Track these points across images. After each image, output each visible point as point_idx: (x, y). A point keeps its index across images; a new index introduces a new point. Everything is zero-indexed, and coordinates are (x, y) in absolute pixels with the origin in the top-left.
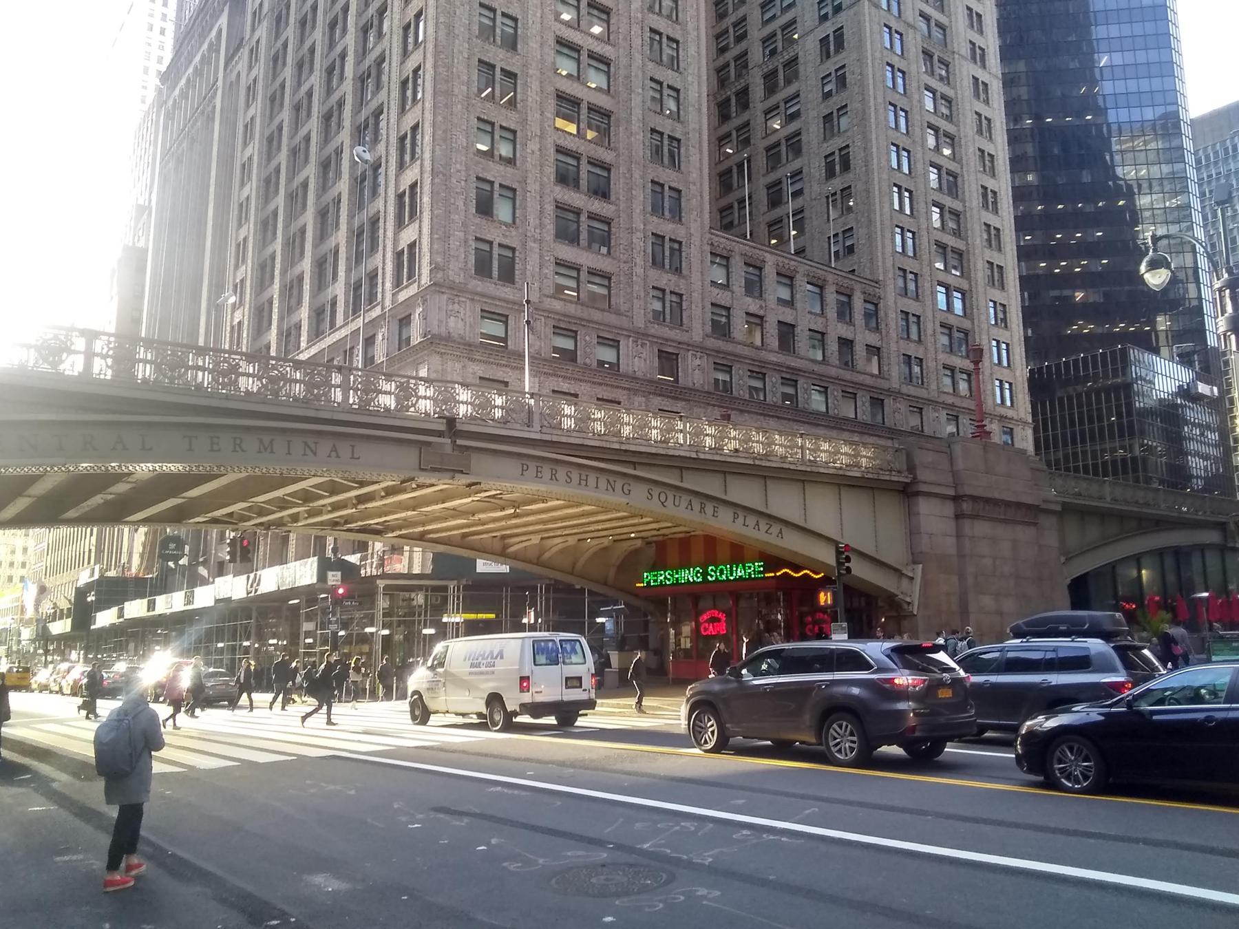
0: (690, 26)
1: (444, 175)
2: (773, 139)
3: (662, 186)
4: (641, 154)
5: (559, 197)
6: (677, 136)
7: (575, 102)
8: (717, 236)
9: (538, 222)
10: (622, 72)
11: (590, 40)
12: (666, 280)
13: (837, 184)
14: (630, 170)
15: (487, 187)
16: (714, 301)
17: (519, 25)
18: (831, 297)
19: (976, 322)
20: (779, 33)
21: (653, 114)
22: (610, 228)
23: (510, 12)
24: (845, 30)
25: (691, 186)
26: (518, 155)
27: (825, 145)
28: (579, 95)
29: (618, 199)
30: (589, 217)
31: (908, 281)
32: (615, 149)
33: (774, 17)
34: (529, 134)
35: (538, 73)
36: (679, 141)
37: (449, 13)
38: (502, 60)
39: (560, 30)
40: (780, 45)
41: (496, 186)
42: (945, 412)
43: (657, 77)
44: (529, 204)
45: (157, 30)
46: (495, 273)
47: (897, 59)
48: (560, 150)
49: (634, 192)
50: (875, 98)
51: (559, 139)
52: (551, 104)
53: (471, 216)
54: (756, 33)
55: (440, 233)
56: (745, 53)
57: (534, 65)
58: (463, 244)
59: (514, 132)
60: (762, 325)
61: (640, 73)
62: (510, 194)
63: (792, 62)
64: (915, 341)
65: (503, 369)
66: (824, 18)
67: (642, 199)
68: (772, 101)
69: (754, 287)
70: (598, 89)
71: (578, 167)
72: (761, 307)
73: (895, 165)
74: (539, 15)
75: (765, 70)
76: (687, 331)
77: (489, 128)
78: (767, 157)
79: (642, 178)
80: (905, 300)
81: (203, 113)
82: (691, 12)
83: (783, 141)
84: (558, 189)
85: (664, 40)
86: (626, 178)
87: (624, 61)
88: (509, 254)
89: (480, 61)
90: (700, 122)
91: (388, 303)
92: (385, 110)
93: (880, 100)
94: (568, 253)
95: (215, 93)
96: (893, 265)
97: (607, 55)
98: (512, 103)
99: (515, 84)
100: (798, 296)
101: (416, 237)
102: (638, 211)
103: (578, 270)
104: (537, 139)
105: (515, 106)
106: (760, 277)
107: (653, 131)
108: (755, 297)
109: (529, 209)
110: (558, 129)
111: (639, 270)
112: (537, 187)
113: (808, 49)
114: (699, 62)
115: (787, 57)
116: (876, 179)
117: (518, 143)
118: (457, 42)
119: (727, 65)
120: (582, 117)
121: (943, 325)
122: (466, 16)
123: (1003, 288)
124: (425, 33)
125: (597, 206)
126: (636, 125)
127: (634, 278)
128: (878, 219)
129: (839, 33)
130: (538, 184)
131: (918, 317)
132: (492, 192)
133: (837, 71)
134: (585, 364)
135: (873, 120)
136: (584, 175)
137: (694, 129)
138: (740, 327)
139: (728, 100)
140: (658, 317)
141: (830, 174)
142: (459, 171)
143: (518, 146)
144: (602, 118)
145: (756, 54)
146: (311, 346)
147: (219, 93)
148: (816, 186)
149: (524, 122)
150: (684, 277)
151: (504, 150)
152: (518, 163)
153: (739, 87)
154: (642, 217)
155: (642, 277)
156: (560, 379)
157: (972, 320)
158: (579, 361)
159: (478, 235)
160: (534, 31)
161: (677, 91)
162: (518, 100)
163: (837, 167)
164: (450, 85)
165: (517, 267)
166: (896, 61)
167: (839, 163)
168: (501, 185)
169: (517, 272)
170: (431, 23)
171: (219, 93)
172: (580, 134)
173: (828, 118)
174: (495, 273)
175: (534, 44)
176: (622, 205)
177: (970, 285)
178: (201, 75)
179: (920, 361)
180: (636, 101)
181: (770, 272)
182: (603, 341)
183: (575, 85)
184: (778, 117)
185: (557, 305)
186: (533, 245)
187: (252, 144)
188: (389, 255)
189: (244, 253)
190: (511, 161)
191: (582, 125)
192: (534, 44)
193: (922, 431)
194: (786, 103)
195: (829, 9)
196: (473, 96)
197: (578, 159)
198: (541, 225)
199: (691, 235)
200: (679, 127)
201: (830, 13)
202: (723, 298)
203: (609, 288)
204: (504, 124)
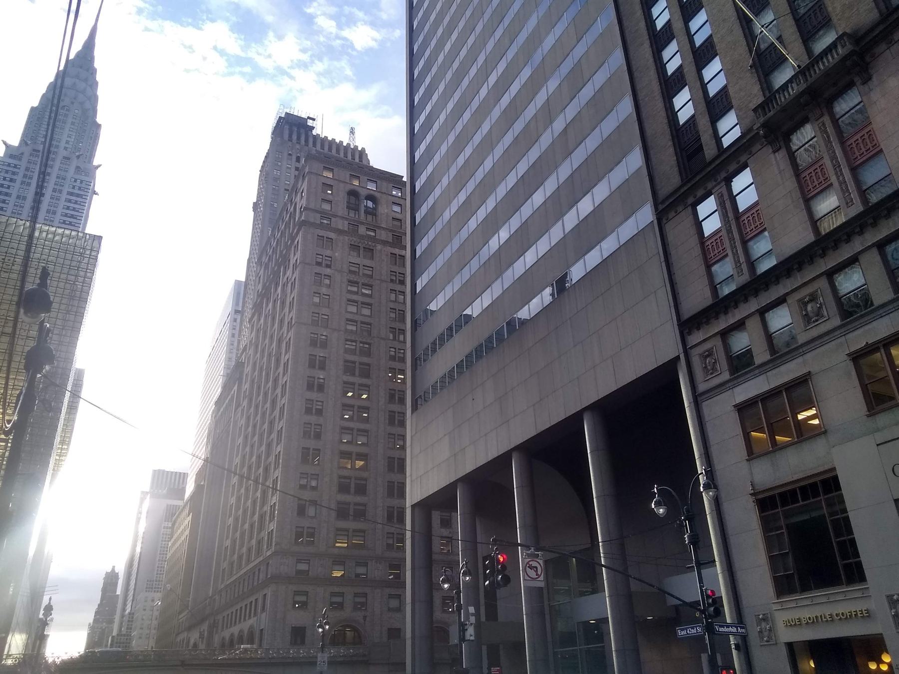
17: (323, 427)
26: (319, 485)
70: (363, 444)
72: (450, 532)
94: (342, 524)
95: (231, 422)
103: (348, 531)
107: (389, 458)
117: (319, 480)
127: (377, 530)
136: (353, 486)
151: (314, 483)
172: (353, 467)
182: (358, 564)
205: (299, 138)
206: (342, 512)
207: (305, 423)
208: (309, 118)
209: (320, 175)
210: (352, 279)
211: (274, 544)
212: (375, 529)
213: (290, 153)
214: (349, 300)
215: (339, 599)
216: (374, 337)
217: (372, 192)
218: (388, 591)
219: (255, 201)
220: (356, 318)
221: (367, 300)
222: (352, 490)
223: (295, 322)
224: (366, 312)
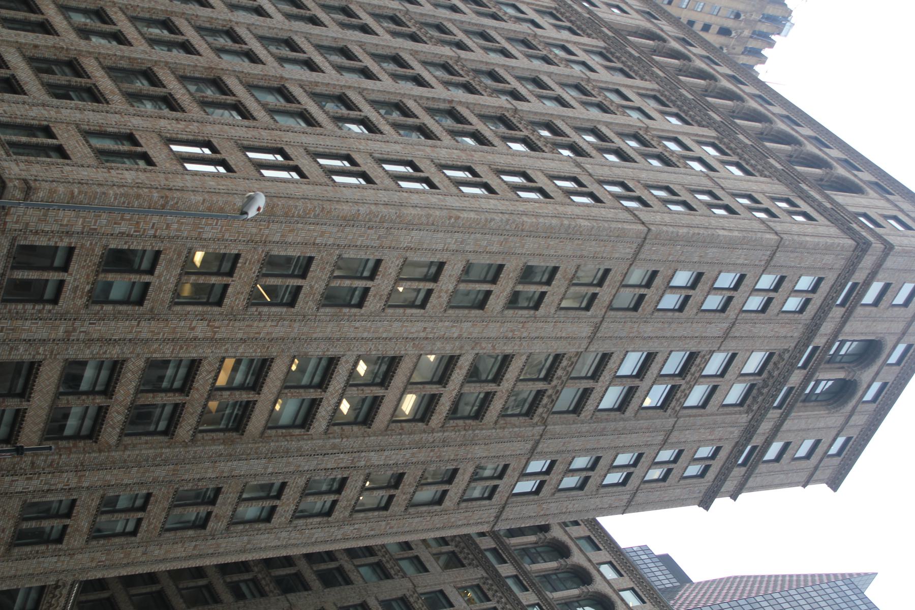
0: (348, 530)
1: (163, 206)
4: (186, 477)
5: (130, 365)
6: (211, 524)
7: (256, 386)
8: (70, 593)
9: (95, 336)
10: (294, 445)
11: (333, 401)
14: (166, 462)
15: (145, 265)
17: (354, 310)
21: (239, 488)
23: (370, 298)
25: (141, 550)
28: (265, 389)
29: (126, 448)
30: (100, 408)
32: (193, 440)
34: (216, 324)
35: (292, 335)
37: (370, 221)
38: (312, 287)
39: (347, 362)
41: (146, 278)
43: (287, 490)
44: (120, 324)
46: (20, 275)
48: (194, 365)
49: (135, 470)
51: (210, 364)
52: (256, 352)
53: (104, 242)
55: (82, 197)
57: (305, 329)
58: (65, 229)
61: (292, 468)
67: (126, 481)
74: (365, 335)
79: (155, 481)
82: (365, 529)
84: (141, 363)
85: (333, 497)
86: (154, 459)
87: (307, 445)
88: (49, 293)
89: (310, 259)
90: (227, 553)
92: (246, 122)
97: (316, 424)
99: (281, 304)
102: (108, 477)
104: (209, 334)
107: (218, 491)
109: (113, 323)
110: (222, 361)
111: (20, 484)
112: (145, 335)
114: (305, 545)
117: (205, 308)
118: (335, 230)
120: (237, 393)
122: (368, 243)
124: (345, 185)
125: (116, 417)
126: (225, 467)
130: (149, 335)
136: (160, 399)
137: (218, 546)
149: (233, 317)
150: (8, 550)
153: (263, 582)
154: (99, 483)
155: (12, 489)
159: (77, 251)
160: (346, 329)
161: (268, 519)
162: (261, 309)
164: (282, 219)
165: (29, 306)
168: (147, 285)
169: (20, 306)
170: (357, 194)
172: (215, 390)
174: (20, 275)
175: (330, 329)
176: (116, 455)
180: (257, 466)
183: (278, 384)
186: (62, 329)
191: (226, 394)
192: (330, 329)
196: (267, 249)
198: (90, 342)
199: (71, 555)
200: (222, 525)
204: (230, 290)
213: (742, 17)
216: (545, 423)
217: (860, 393)
222: (148, 399)
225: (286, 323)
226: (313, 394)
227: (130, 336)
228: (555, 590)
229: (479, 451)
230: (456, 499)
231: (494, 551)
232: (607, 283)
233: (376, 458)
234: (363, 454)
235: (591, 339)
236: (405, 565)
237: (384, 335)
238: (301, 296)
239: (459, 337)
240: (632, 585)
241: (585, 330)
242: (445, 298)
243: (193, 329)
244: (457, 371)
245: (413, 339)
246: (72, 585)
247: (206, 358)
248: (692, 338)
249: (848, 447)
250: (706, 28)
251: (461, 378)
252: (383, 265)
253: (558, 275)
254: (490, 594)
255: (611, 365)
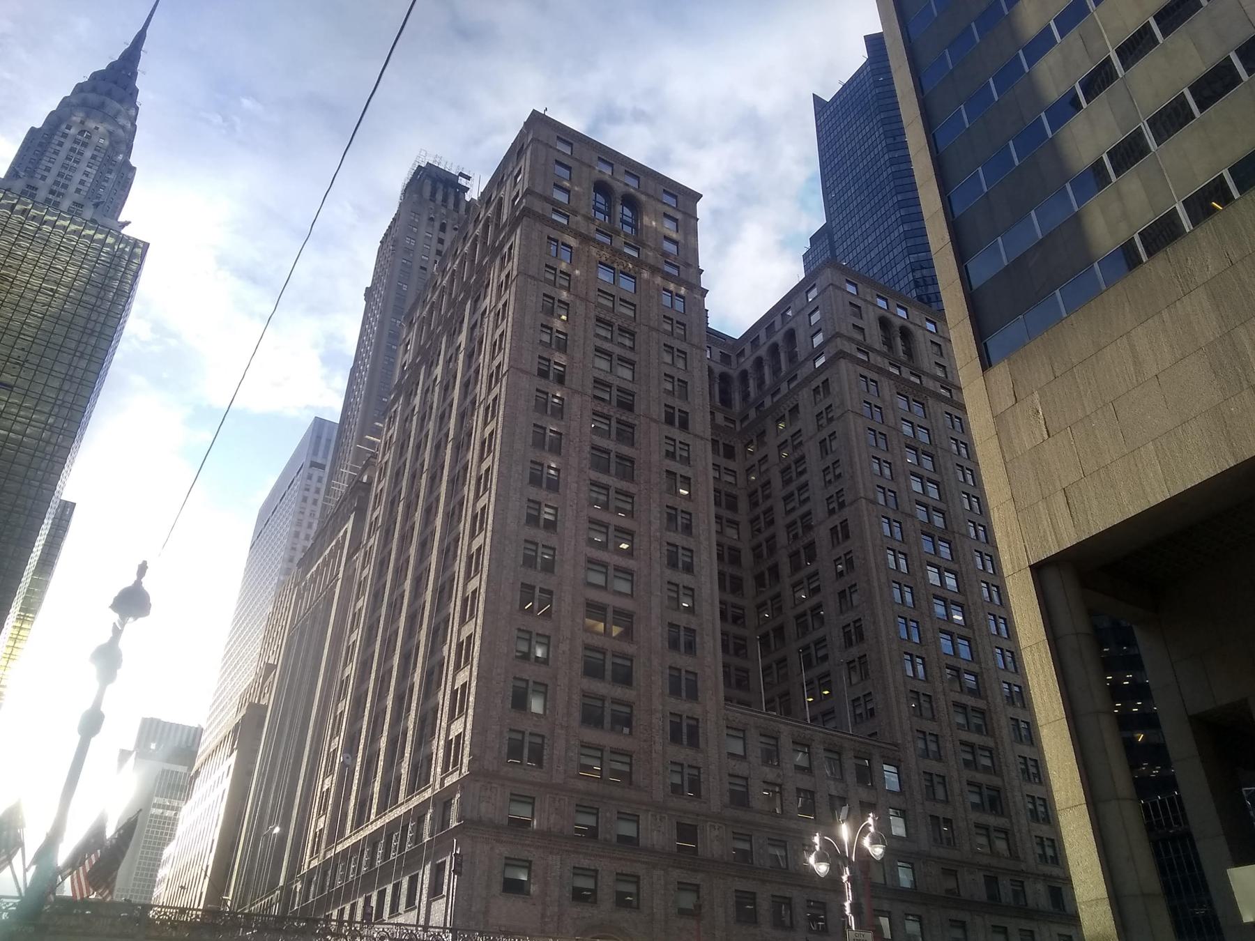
2: (800, 610)
3: (679, 670)
6: (693, 627)
12: (683, 754)
13: (855, 652)
16: (731, 772)
18: (849, 763)
19: (1006, 778)
20: (799, 521)
22: (632, 711)
24: (848, 522)
26: (551, 656)
27: (842, 617)
31: (928, 743)
33: (793, 509)
36: (694, 631)
40: (800, 531)
41: (531, 683)
42: (981, 874)
45: (310, 501)
47: (897, 543)
49: (653, 678)
50: (879, 579)
54: (781, 521)
56: (773, 537)
59: (548, 637)
60: (780, 792)
62: (542, 689)
63: (811, 546)
64: (942, 801)
65: (529, 849)
66: (832, 512)
67: (660, 683)
68: (797, 577)
69: (771, 756)
71: (604, 660)
72: (779, 776)
73: (904, 636)
74: (573, 543)
75: (790, 551)
76: (705, 803)
77: (527, 636)
78: (797, 624)
80: (927, 761)
81: (325, 597)
83: (809, 612)
88: (539, 740)
91: (437, 786)
93: (883, 579)
94: (592, 735)
96: (911, 728)
97: (631, 567)
98: (548, 614)
100: (815, 763)
101: (462, 730)
103: (602, 751)
104: (568, 641)
105: (550, 617)
106: (777, 746)
107: (671, 625)
108: (772, 766)
111: (658, 747)
113: (822, 534)
115: (806, 541)
116: (886, 649)
119: (760, 545)
121: (970, 783)
123: (1032, 743)
127: (654, 755)
128: (892, 685)
129: (844, 524)
131: (943, 778)
132: (527, 688)
133: (845, 555)
134: (605, 840)
135: (878, 598)
136: (609, 666)
138: (760, 794)
139: (762, 574)
140: (676, 789)
141: (849, 643)
142: (499, 674)
143: (551, 649)
144: (624, 617)
145: (782, 538)
146: (378, 819)
147: (339, 583)
148: (838, 655)
152: (550, 663)
156: (581, 856)
157: (1002, 777)
158: (599, 837)
159: (512, 728)
163: (853, 637)
165: (545, 752)
166: (896, 545)
167: (854, 634)
168: (535, 683)
169: (545, 757)
171: (339, 583)
172: (607, 633)
173: (842, 594)
177: (996, 743)
178: (328, 566)
179: (948, 822)
181: (786, 742)
182: (622, 816)
184: (803, 591)
185: (581, 785)
186: (560, 731)
187: (356, 631)
188: (442, 743)
189: (339, 725)
190: (544, 661)
193: (959, 895)
194: (808, 579)
195: (835, 505)
197: (604, 654)
201: (837, 507)
202: (741, 768)
203: (630, 765)
204: (540, 632)
205: (445, 200)
206: (591, 717)
207: (526, 541)
208: (461, 174)
209: (551, 147)
210: (602, 316)
211: (466, 761)
212: (651, 752)
213: (432, 216)
214: (597, 349)
215: (588, 884)
218: (677, 874)
219: (369, 286)
220: (610, 379)
221: (628, 355)
222: (608, 674)
223: (510, 367)
224: (626, 373)
225: (563, 594)
226: (611, 571)
227: (567, 690)
228: (780, 368)
229: (655, 458)
230: (688, 468)
231: (773, 395)
232: (546, 390)
233: (656, 525)
234: (652, 534)
235: (583, 394)
236: (763, 468)
237: (574, 531)
238: (546, 587)
239: (577, 483)
240: (804, 293)
241: (577, 398)
242: (551, 495)
243: (564, 652)
244: (600, 480)
245: (577, 512)
246: (727, 710)
247: (583, 641)
248: (585, 324)
249: (672, 192)
250: (441, 241)
251: (606, 476)
252: (528, 539)
253: (539, 423)
254: (781, 415)
255: (602, 376)
